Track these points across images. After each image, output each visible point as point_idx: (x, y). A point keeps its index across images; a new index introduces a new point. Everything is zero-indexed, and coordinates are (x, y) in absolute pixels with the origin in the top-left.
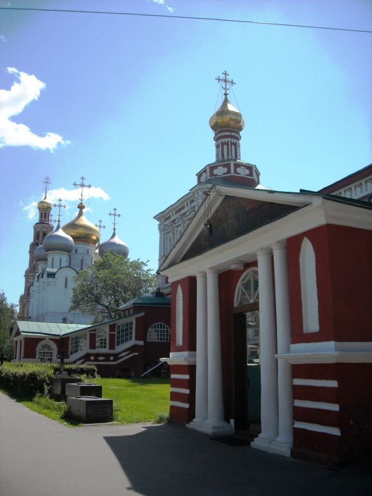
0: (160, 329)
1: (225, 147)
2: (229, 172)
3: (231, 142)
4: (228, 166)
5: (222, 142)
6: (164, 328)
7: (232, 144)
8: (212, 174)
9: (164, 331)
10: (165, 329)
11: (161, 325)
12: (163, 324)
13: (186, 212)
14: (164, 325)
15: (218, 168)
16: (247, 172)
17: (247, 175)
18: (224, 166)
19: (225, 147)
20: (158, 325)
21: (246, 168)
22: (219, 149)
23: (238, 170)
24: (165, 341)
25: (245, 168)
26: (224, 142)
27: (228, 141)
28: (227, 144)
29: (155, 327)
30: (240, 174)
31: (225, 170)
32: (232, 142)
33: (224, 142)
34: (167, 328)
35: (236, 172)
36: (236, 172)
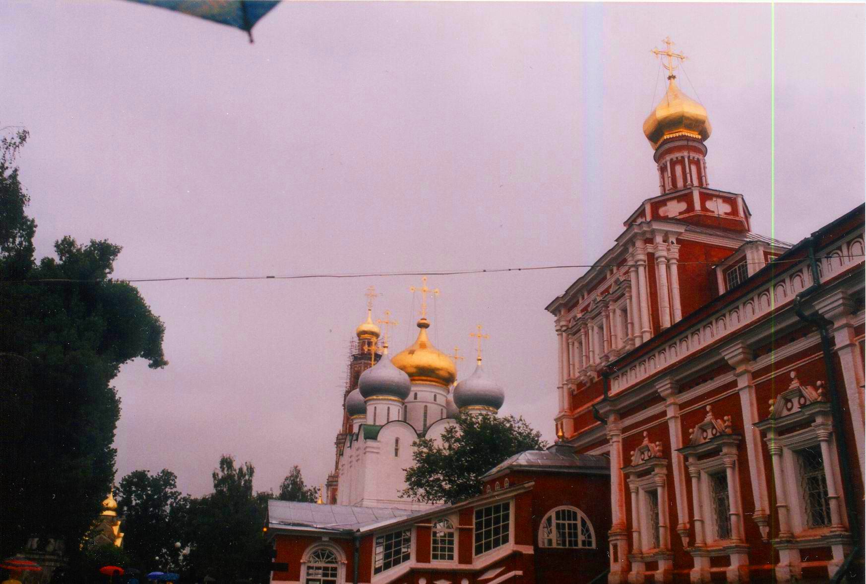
1: (678, 169)
5: (671, 160)
8: (656, 217)
13: (610, 287)
18: (680, 199)
19: (678, 169)
26: (675, 159)
27: (683, 157)
28: (681, 161)
31: (683, 206)
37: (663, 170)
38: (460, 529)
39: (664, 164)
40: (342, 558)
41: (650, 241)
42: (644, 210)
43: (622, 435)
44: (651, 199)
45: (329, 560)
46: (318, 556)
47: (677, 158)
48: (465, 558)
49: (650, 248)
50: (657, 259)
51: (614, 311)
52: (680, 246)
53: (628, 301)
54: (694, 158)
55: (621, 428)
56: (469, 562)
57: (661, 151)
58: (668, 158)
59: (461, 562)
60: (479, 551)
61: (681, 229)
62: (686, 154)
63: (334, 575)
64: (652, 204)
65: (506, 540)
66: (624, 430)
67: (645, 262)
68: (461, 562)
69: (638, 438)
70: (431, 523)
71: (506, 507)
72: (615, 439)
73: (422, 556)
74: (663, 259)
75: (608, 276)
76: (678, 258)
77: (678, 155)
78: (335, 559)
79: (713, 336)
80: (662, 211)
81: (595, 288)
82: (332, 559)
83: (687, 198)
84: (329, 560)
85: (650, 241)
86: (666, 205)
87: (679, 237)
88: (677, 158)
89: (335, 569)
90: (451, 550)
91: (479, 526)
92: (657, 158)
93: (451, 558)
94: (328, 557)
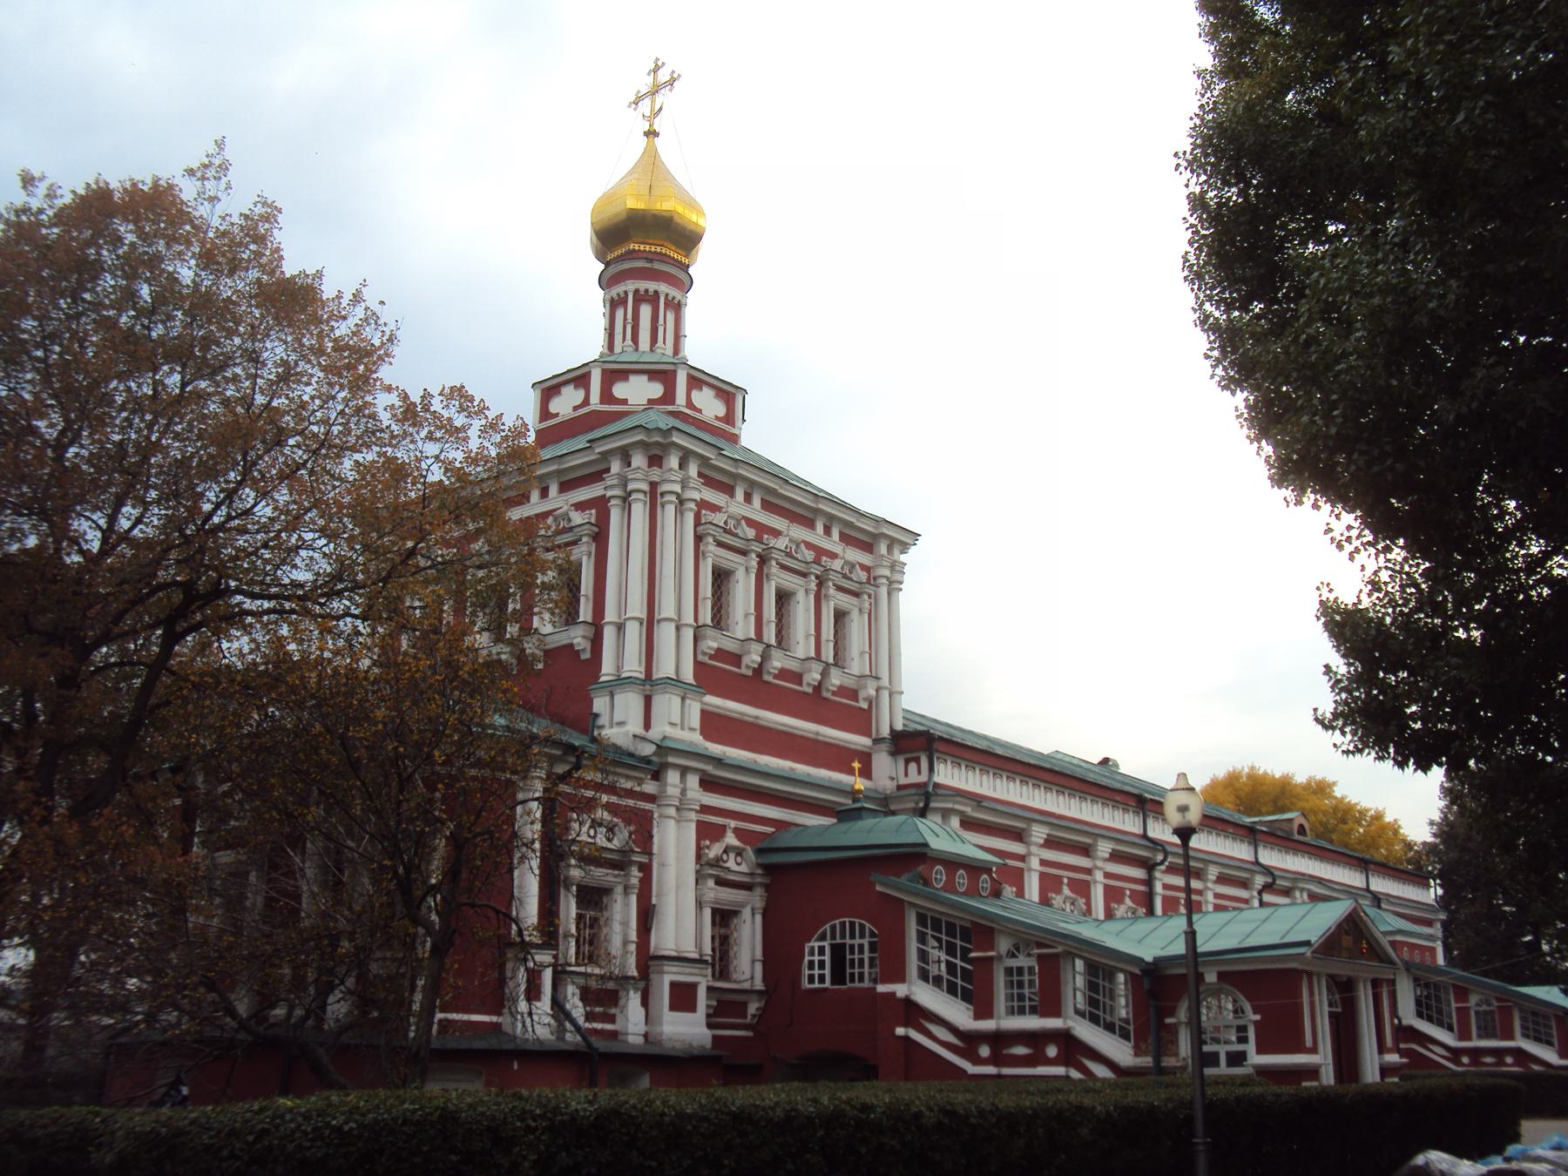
1: (646, 311)
2: (669, 397)
4: (664, 376)
5: (637, 291)
8: (607, 397)
15: (632, 378)
16: (721, 411)
17: (717, 418)
18: (654, 375)
19: (646, 311)
22: (620, 313)
28: (653, 299)
30: (700, 411)
31: (657, 390)
35: (690, 404)
57: (614, 269)
62: (663, 288)
64: (604, 372)
77: (652, 286)
80: (619, 390)
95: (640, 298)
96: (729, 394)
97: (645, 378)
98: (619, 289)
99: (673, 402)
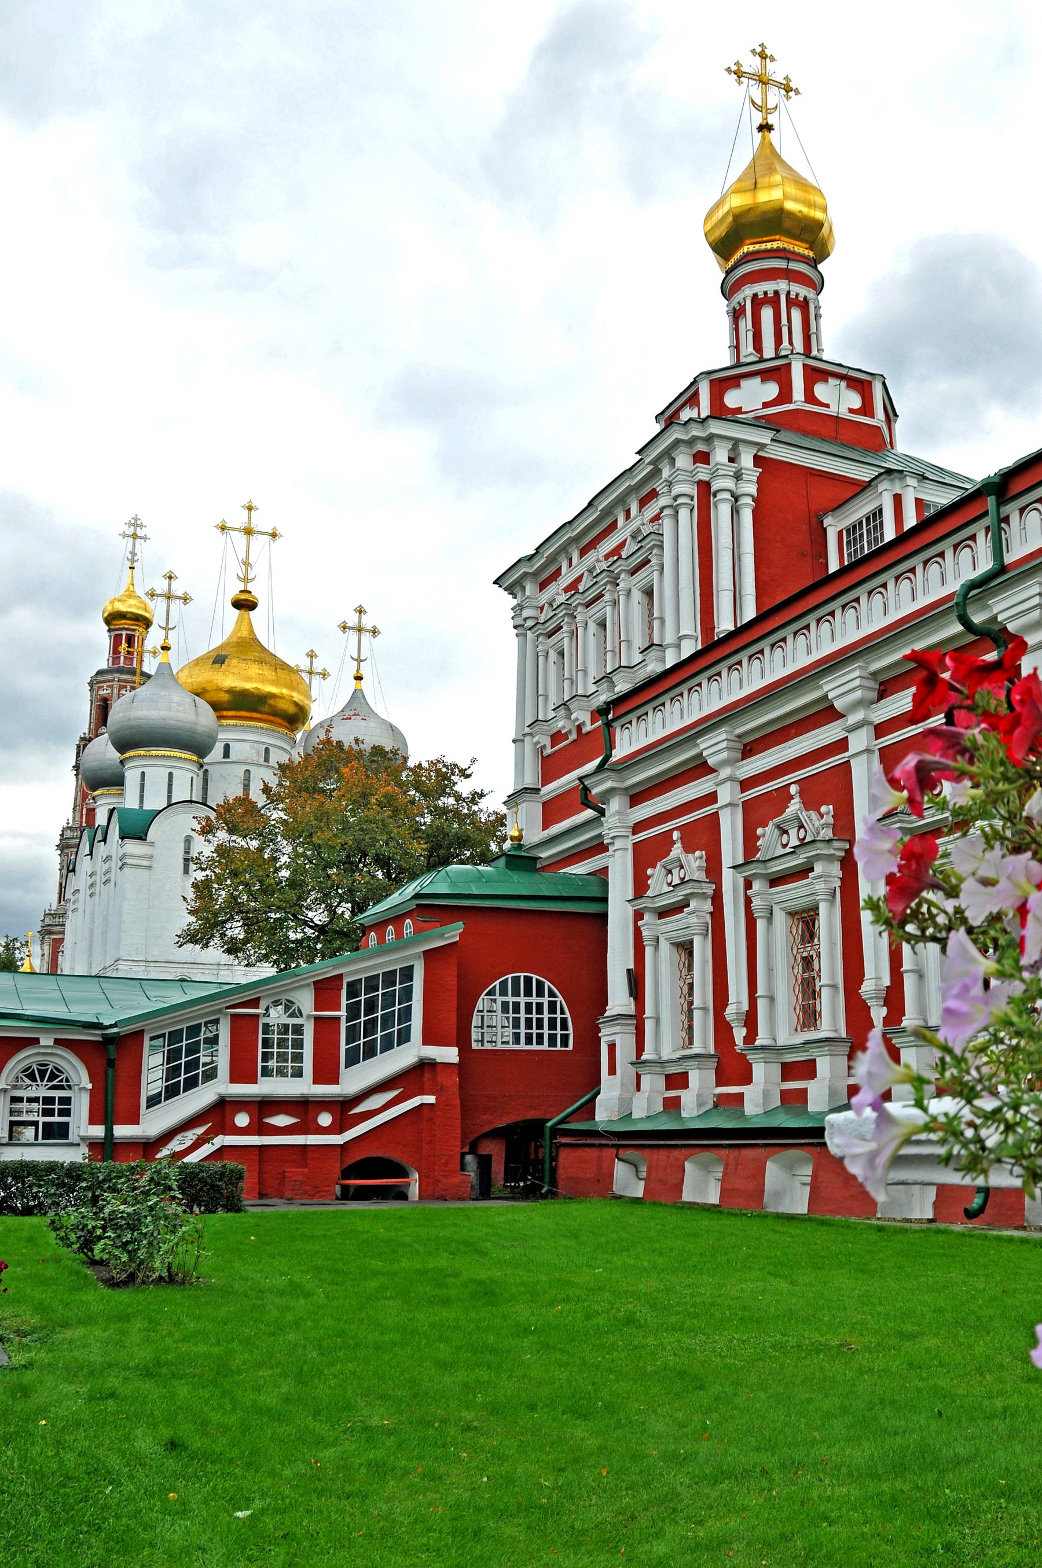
0: (523, 1000)
1: (767, 314)
2: (785, 395)
3: (788, 293)
4: (779, 374)
5: (755, 295)
6: (540, 994)
7: (791, 303)
9: (540, 1006)
10: (545, 1000)
11: (528, 981)
12: (535, 977)
13: (623, 544)
14: (540, 984)
15: (745, 383)
17: (851, 411)
18: (766, 375)
19: (767, 314)
20: (516, 981)
21: (848, 386)
23: (821, 391)
24: (545, 1047)
25: (843, 384)
26: (761, 296)
28: (774, 301)
29: (504, 992)
30: (827, 406)
31: (772, 390)
32: (793, 296)
33: (761, 296)
34: (552, 994)
35: (810, 397)
36: (810, 397)
37: (736, 315)
38: (317, 1019)
39: (739, 303)
40: (79, 1075)
41: (702, 458)
42: (696, 394)
43: (632, 837)
44: (709, 373)
45: (55, 1083)
46: (32, 1077)
47: (766, 293)
48: (326, 1073)
49: (703, 473)
50: (715, 496)
51: (629, 592)
52: (760, 470)
53: (656, 574)
54: (797, 295)
55: (631, 824)
56: (335, 1080)
58: (748, 291)
59: (317, 1081)
60: (352, 1060)
61: (764, 437)
62: (782, 286)
63: (66, 1113)
65: (404, 1037)
66: (638, 828)
67: (692, 499)
68: (317, 1081)
69: (664, 842)
70: (258, 1008)
71: (407, 973)
72: (618, 844)
73: (242, 1072)
74: (727, 495)
75: (621, 522)
76: (756, 494)
78: (67, 1080)
79: (809, 652)
80: (732, 399)
81: (592, 545)
82: (61, 1081)
83: (779, 374)
84: (55, 1083)
85: (702, 458)
86: (738, 385)
87: (760, 454)
88: (766, 293)
89: (67, 1101)
90: (298, 1058)
91: (353, 1012)
92: (728, 290)
93: (298, 1073)
94: (52, 1077)
95: (758, 303)
96: (860, 383)
97: (757, 380)
98: (738, 297)
99: (790, 401)
